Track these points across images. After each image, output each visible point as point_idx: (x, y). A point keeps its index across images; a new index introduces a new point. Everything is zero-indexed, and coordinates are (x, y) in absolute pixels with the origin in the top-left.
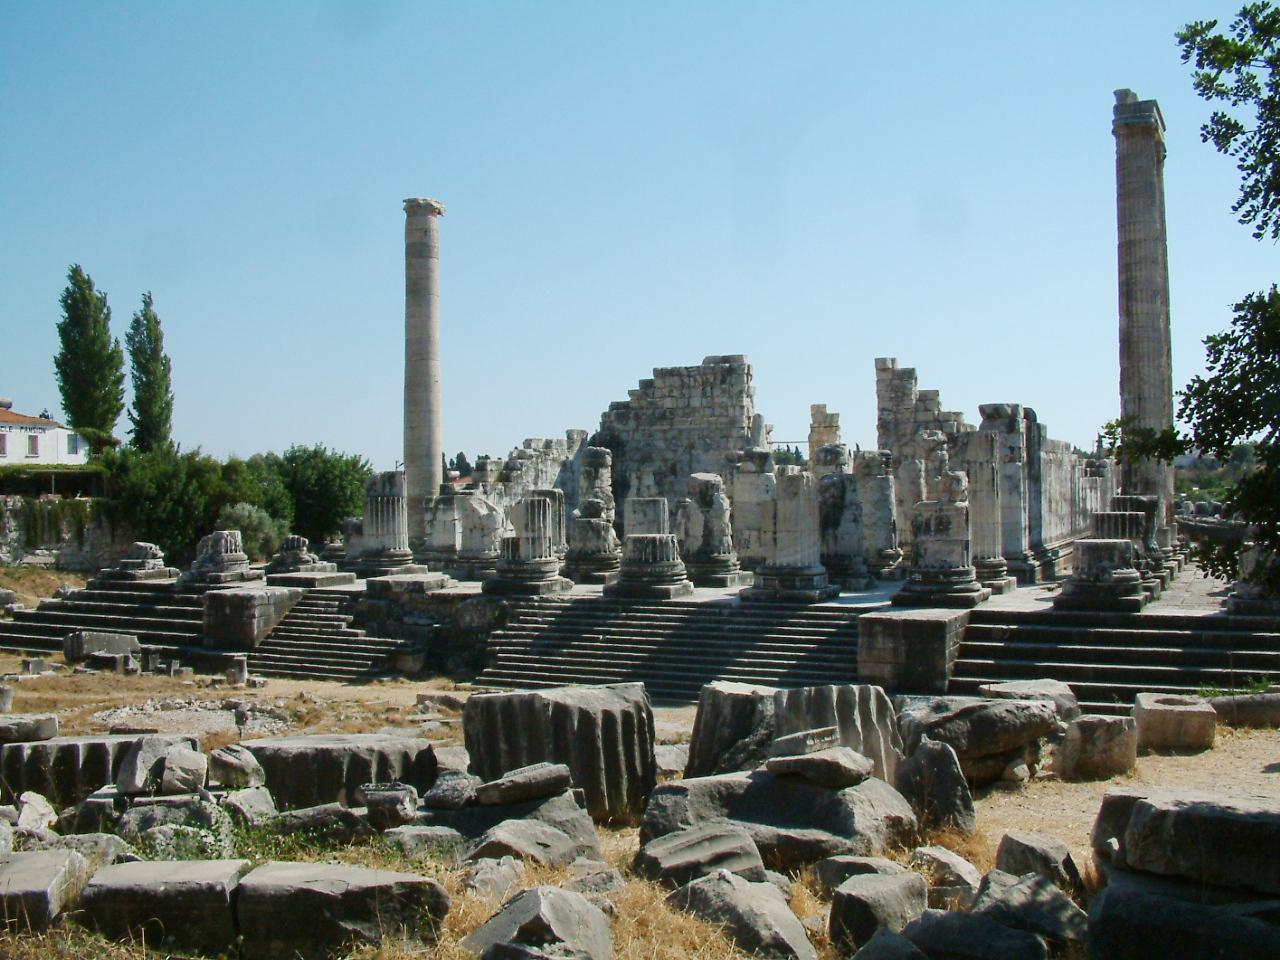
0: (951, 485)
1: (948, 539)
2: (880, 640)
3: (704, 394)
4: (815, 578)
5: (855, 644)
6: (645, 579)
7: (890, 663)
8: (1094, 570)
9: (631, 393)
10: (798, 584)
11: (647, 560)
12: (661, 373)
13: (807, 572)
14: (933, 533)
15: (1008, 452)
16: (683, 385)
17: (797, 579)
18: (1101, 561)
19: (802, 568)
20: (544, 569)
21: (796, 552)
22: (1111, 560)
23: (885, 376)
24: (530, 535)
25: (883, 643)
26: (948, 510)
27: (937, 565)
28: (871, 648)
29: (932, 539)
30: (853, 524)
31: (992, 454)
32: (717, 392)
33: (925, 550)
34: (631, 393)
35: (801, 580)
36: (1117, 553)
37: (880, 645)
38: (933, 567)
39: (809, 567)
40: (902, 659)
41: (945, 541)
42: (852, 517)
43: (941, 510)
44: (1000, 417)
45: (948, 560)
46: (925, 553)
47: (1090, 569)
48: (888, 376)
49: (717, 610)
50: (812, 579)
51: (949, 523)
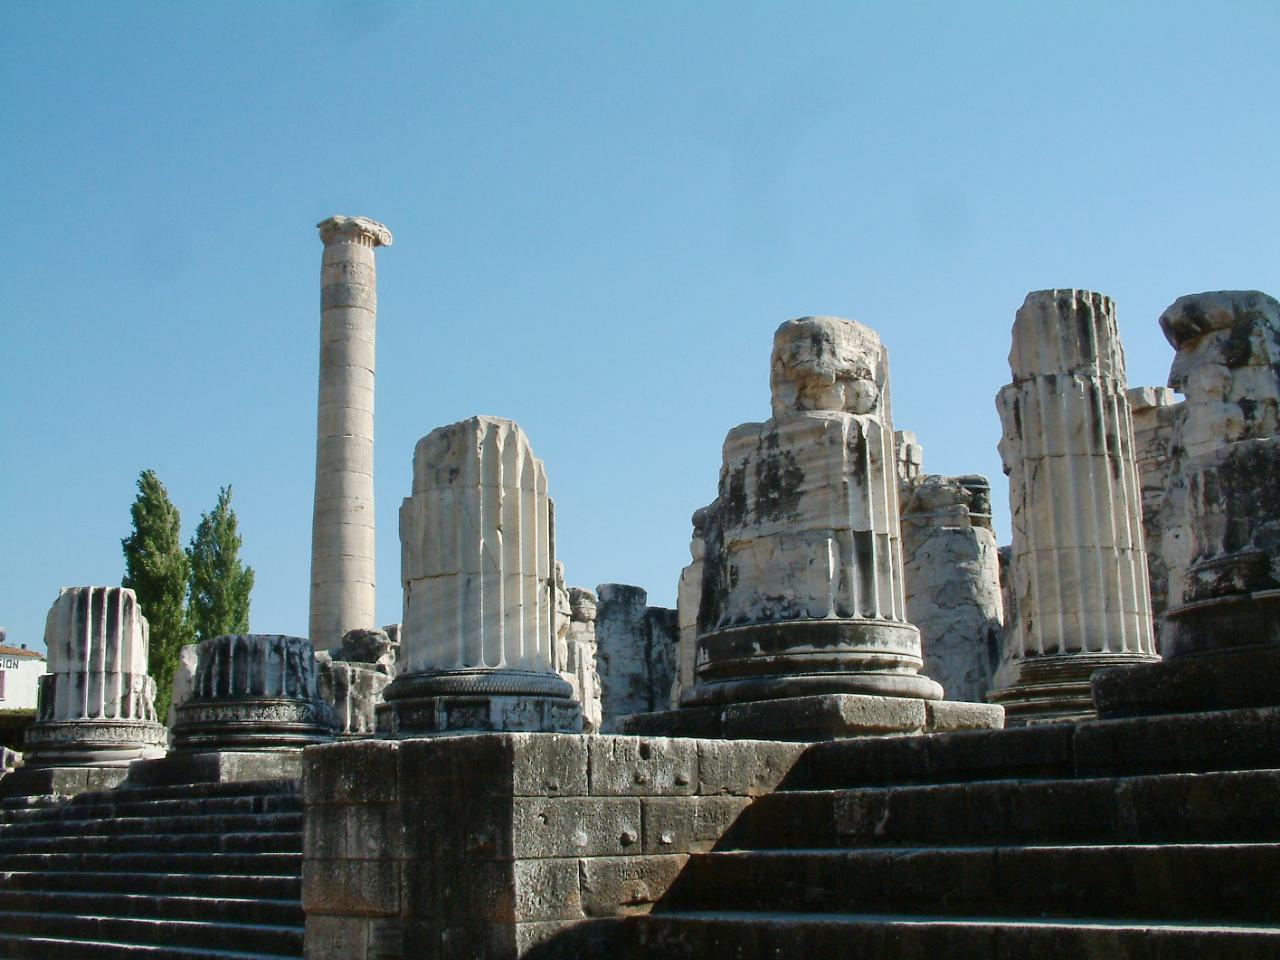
0: (794, 356)
1: (796, 529)
2: (351, 824)
4: (497, 703)
5: (296, 844)
6: (193, 739)
7: (374, 915)
8: (1249, 548)
10: (441, 717)
11: (208, 692)
14: (751, 517)
15: (1237, 414)
20: (92, 738)
21: (452, 631)
23: (1151, 422)
24: (75, 665)
25: (359, 839)
26: (791, 438)
27: (752, 613)
28: (330, 860)
29: (747, 535)
33: (735, 572)
35: (449, 707)
37: (353, 853)
38: (742, 620)
40: (400, 904)
41: (781, 538)
43: (773, 440)
44: (1206, 328)
45: (789, 594)
46: (734, 583)
47: (1231, 544)
48: (1151, 422)
49: (251, 799)
50: (487, 704)
51: (797, 476)
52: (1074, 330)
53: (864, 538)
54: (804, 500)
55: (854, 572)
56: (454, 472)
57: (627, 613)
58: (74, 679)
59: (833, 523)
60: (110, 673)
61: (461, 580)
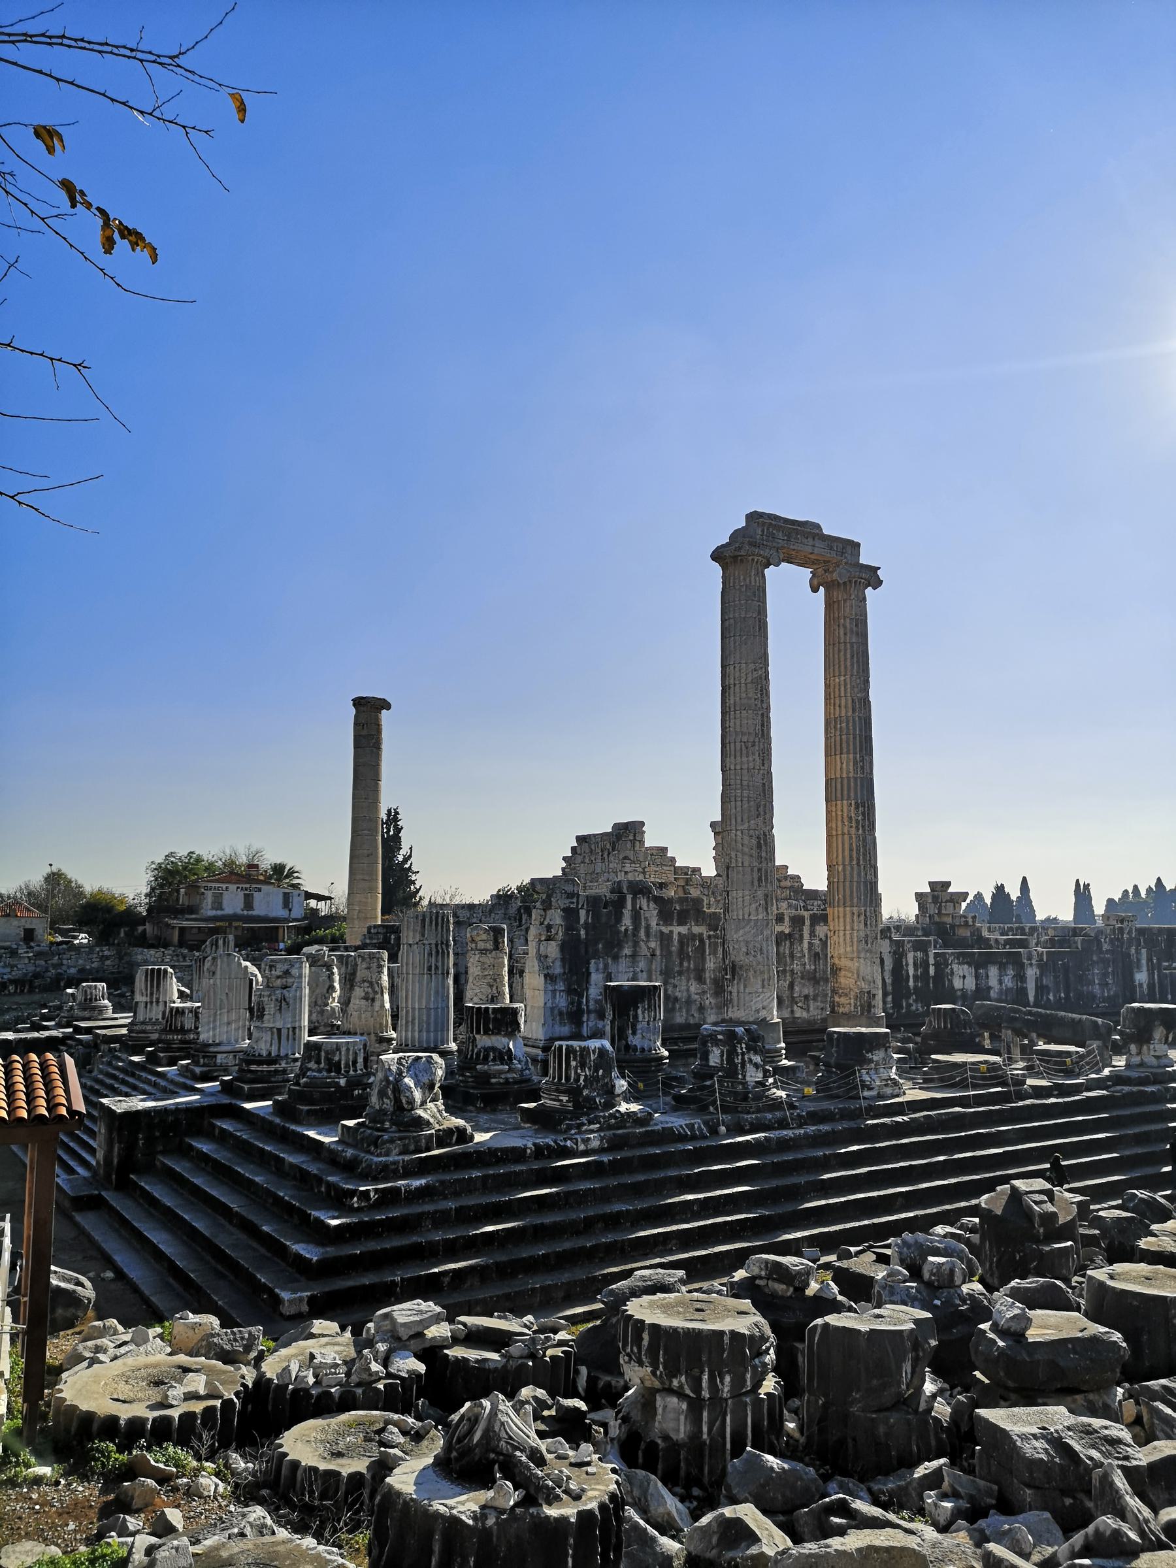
3: (603, 859)
4: (219, 1056)
9: (564, 859)
12: (581, 839)
13: (212, 1049)
16: (591, 851)
17: (201, 1055)
18: (310, 1061)
19: (210, 1045)
22: (318, 1062)
24: (144, 999)
30: (363, 1002)
31: (423, 935)
32: (612, 858)
34: (564, 859)
35: (204, 1057)
36: (323, 1054)
39: (219, 1044)
42: (363, 994)
51: (264, 1009)
52: (419, 928)
53: (279, 1030)
54: (266, 1017)
55: (276, 1041)
56: (214, 973)
57: (507, 909)
58: (143, 1005)
59: (271, 1025)
60: (158, 1002)
61: (212, 1012)
